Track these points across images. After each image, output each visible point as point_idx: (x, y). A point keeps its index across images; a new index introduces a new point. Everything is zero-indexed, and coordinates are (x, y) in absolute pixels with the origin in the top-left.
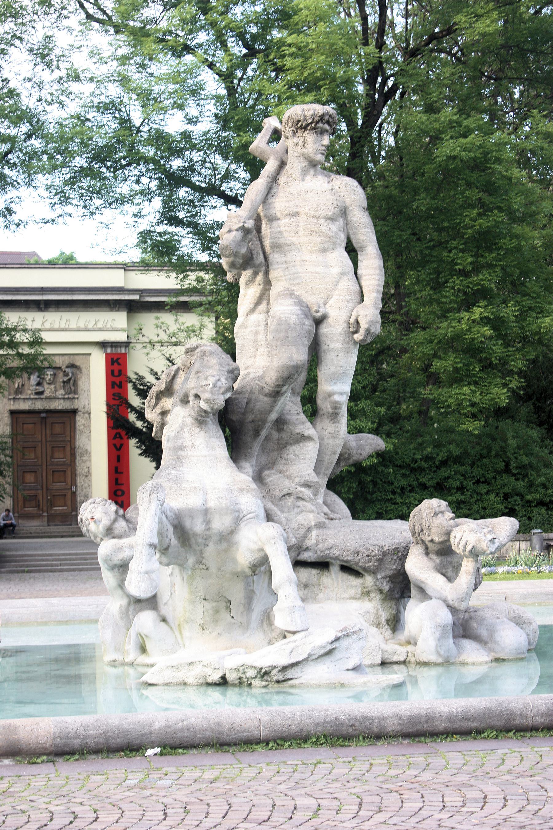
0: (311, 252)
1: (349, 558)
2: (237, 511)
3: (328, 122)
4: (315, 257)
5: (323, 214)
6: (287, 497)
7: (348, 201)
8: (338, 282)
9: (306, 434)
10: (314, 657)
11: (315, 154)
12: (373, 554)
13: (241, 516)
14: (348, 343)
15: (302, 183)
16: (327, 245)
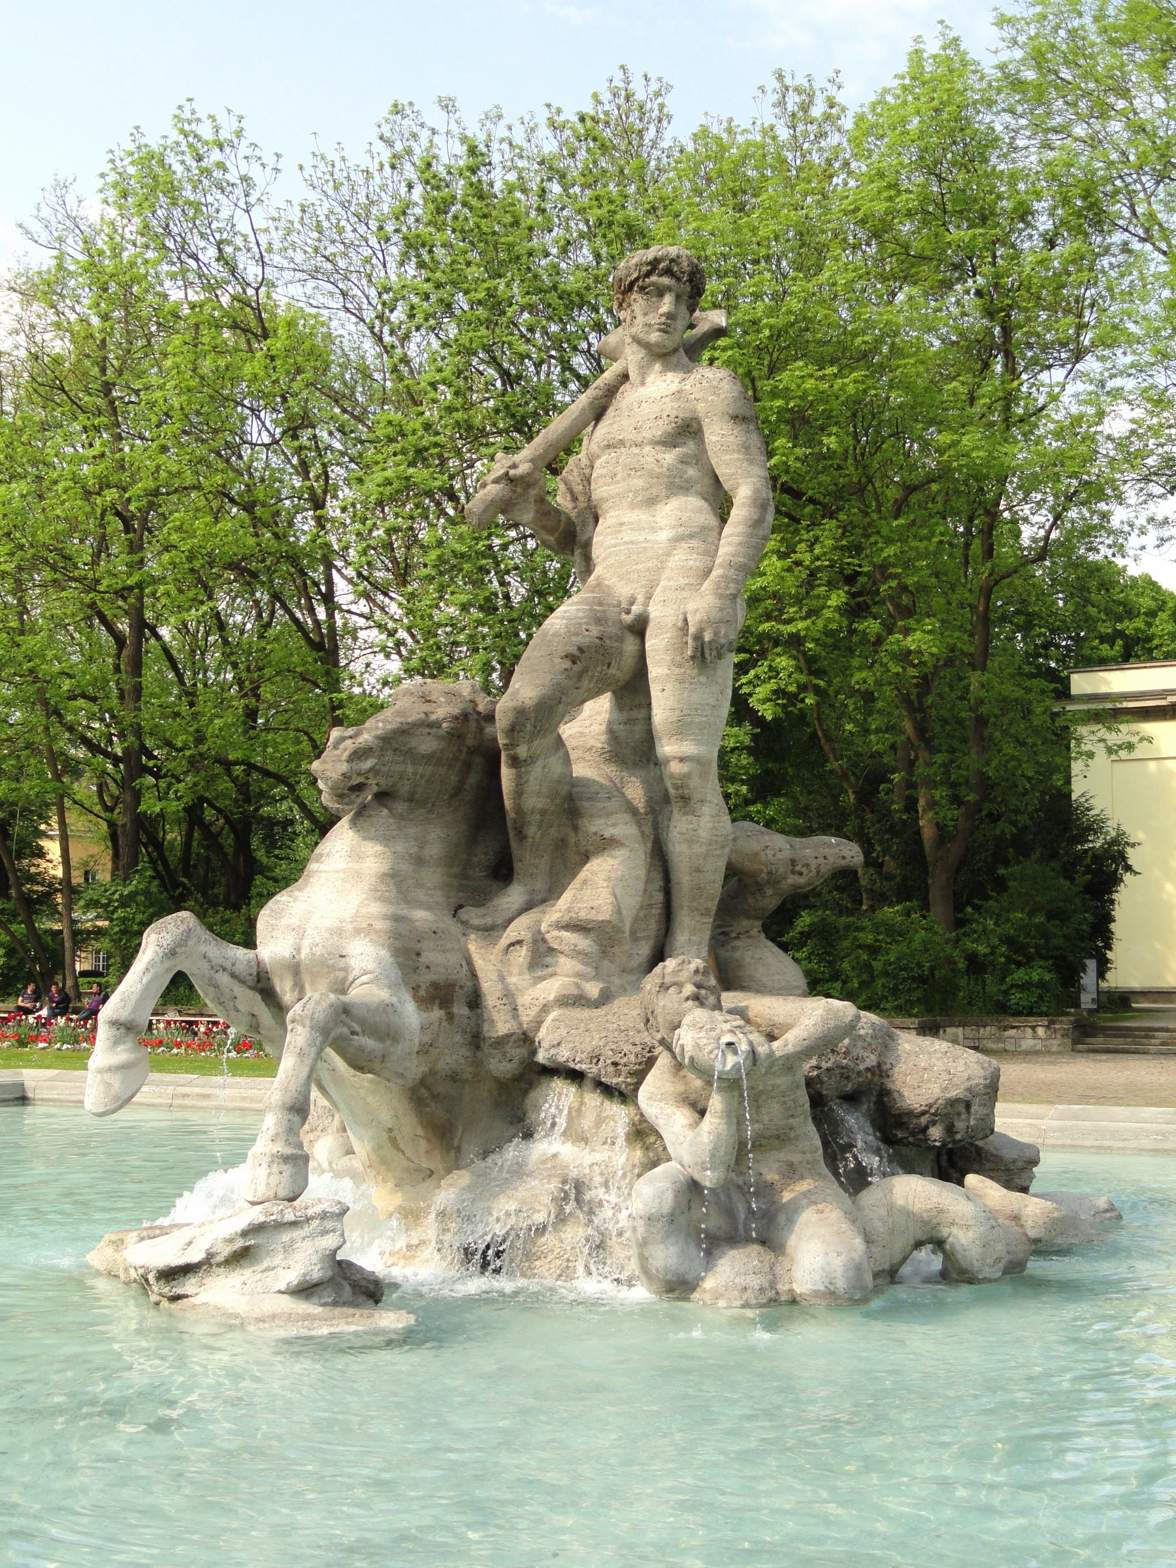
0: (633, 506)
1: (584, 1067)
2: (342, 969)
3: (668, 272)
4: (641, 515)
5: (648, 434)
6: (518, 947)
7: (701, 408)
8: (669, 554)
9: (607, 834)
10: (220, 1258)
11: (648, 333)
12: (625, 1060)
13: (351, 978)
14: (680, 666)
15: (641, 389)
16: (655, 491)
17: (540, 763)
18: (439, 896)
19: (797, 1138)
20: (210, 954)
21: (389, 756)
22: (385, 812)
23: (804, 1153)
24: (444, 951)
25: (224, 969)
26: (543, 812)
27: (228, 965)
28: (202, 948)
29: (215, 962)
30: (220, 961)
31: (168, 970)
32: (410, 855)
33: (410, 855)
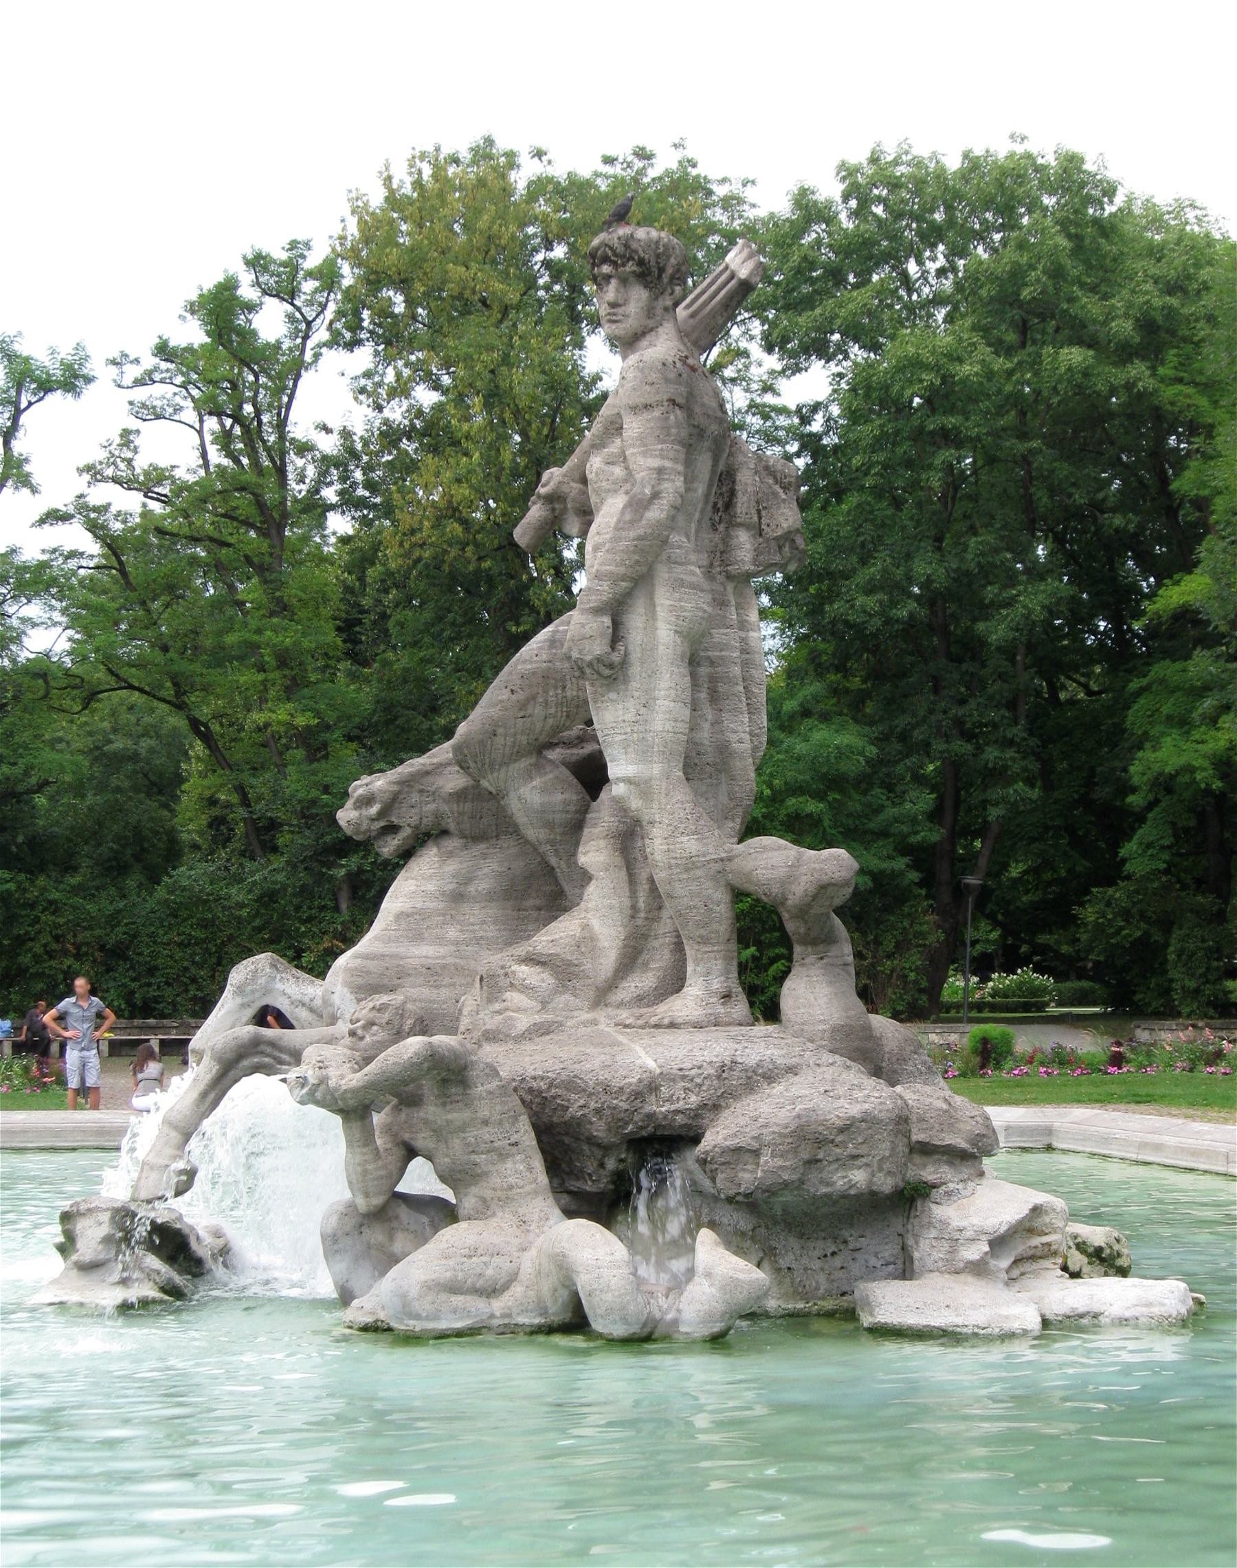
17: (512, 795)
18: (491, 931)
19: (486, 1174)
20: (288, 991)
21: (415, 797)
22: (435, 850)
23: (494, 1189)
24: (437, 987)
25: (304, 1005)
26: (552, 843)
27: (306, 1000)
28: (279, 986)
29: (294, 997)
30: (299, 997)
31: (243, 1006)
32: (443, 894)
33: (443, 894)
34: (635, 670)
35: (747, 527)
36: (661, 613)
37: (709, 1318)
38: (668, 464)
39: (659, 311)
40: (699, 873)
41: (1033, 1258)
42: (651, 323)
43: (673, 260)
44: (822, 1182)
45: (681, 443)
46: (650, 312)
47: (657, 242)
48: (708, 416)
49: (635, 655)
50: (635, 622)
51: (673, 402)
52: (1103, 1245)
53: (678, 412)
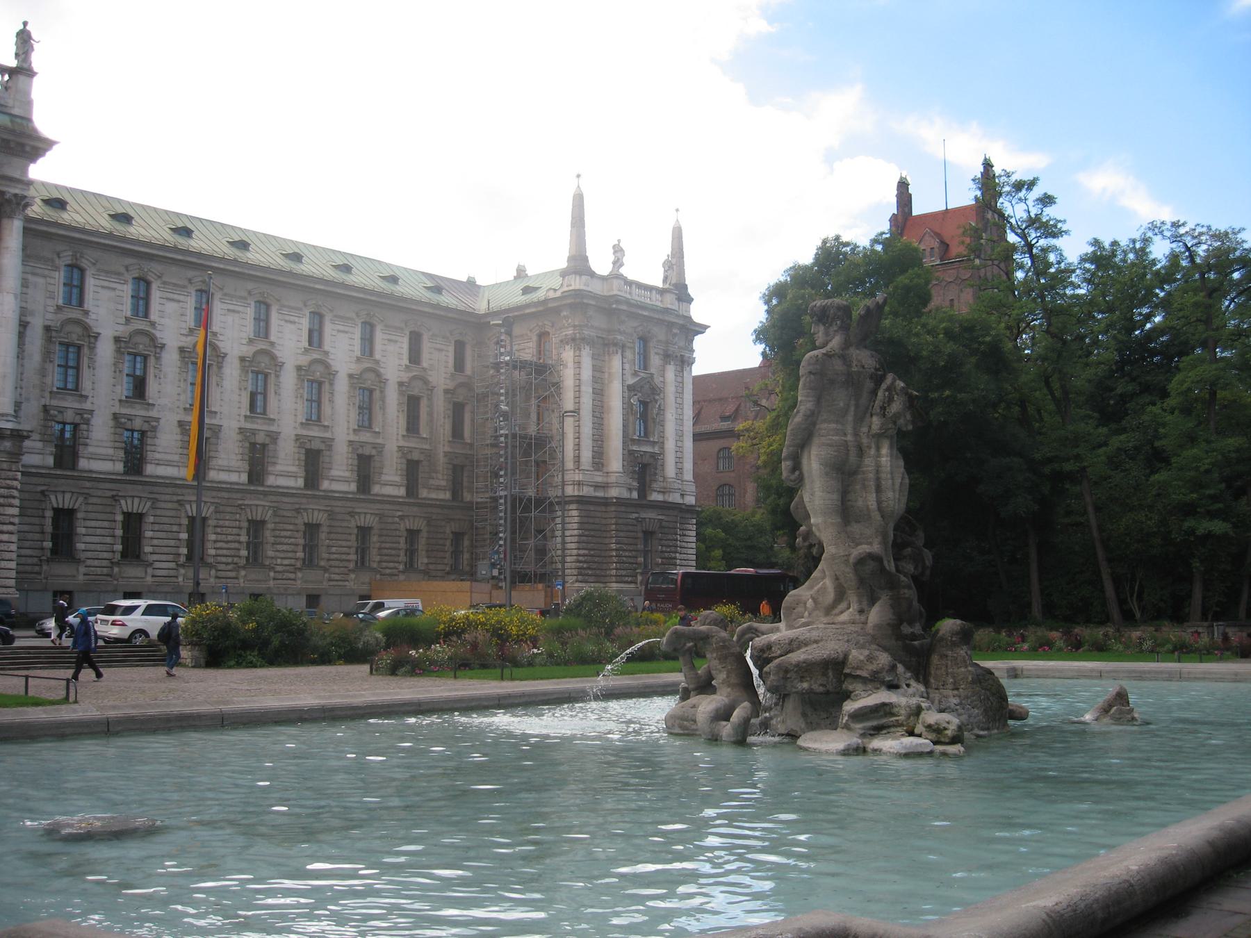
34: (807, 481)
35: (877, 415)
36: (813, 457)
37: (729, 736)
38: (804, 398)
39: (832, 333)
40: (837, 561)
41: (894, 726)
42: (829, 338)
43: (832, 312)
44: (792, 686)
45: (811, 389)
46: (827, 334)
47: (824, 307)
48: (837, 374)
49: (806, 475)
50: (805, 461)
51: (810, 373)
52: (932, 723)
53: (812, 376)
